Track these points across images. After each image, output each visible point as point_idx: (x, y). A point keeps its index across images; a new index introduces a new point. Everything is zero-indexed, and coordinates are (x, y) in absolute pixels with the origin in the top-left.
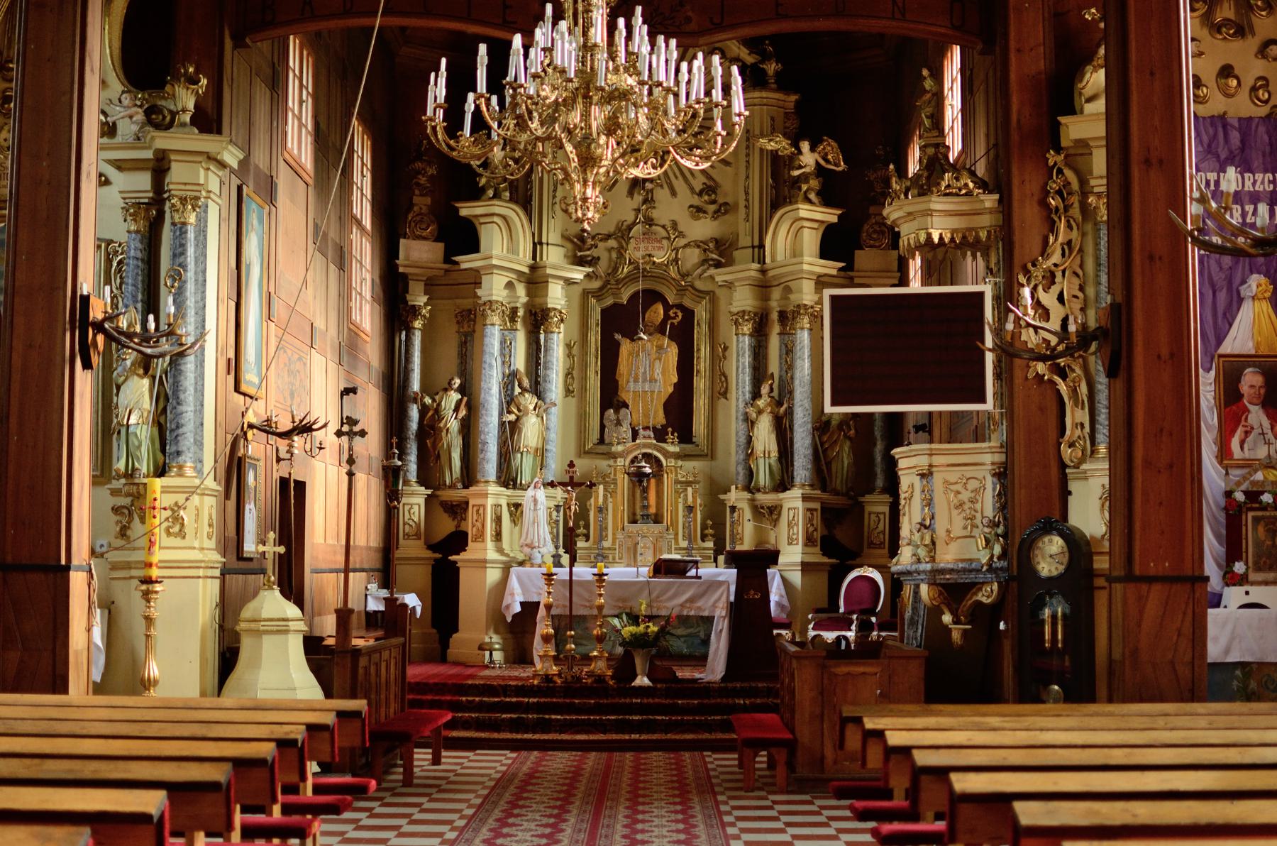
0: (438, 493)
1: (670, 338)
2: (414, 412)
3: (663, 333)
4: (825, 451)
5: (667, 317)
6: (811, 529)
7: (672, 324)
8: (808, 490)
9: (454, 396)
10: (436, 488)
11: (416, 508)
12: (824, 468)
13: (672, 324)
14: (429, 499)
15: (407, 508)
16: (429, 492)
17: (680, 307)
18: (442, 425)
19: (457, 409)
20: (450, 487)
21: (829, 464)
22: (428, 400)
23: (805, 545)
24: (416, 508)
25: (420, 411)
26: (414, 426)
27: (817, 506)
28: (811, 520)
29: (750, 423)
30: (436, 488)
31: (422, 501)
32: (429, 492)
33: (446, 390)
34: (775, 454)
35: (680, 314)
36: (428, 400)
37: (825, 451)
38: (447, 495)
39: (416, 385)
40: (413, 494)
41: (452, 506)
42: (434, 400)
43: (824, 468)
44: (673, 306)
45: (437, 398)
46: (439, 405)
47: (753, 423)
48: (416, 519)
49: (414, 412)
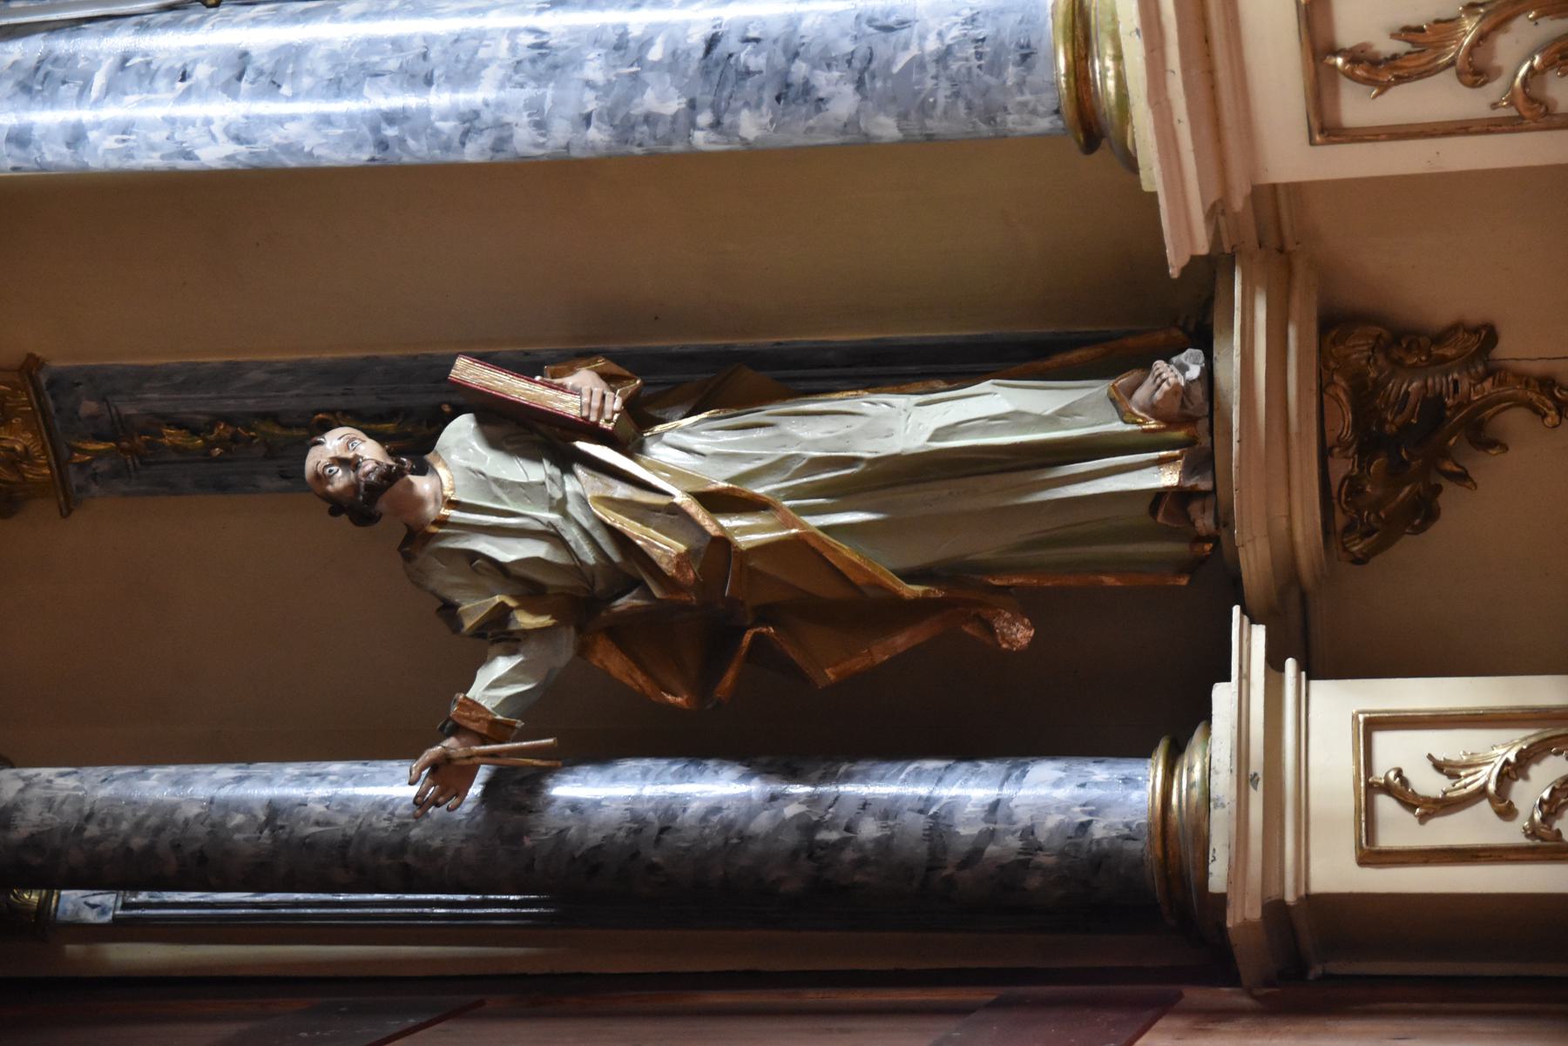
0: (1254, 559)
2: (602, 793)
9: (463, 457)
10: (1226, 586)
11: (1393, 751)
14: (1319, 643)
15: (1398, 828)
16: (1250, 643)
18: (665, 546)
19: (548, 438)
20: (1201, 459)
22: (494, 683)
24: (1399, 753)
25: (600, 751)
26: (717, 789)
30: (1226, 586)
31: (1335, 706)
32: (1250, 643)
33: (418, 537)
36: (494, 683)
38: (1277, 512)
39: (390, 786)
40: (1270, 776)
41: (1368, 441)
42: (497, 634)
45: (474, 608)
46: (525, 583)
48: (1502, 746)
49: (602, 793)
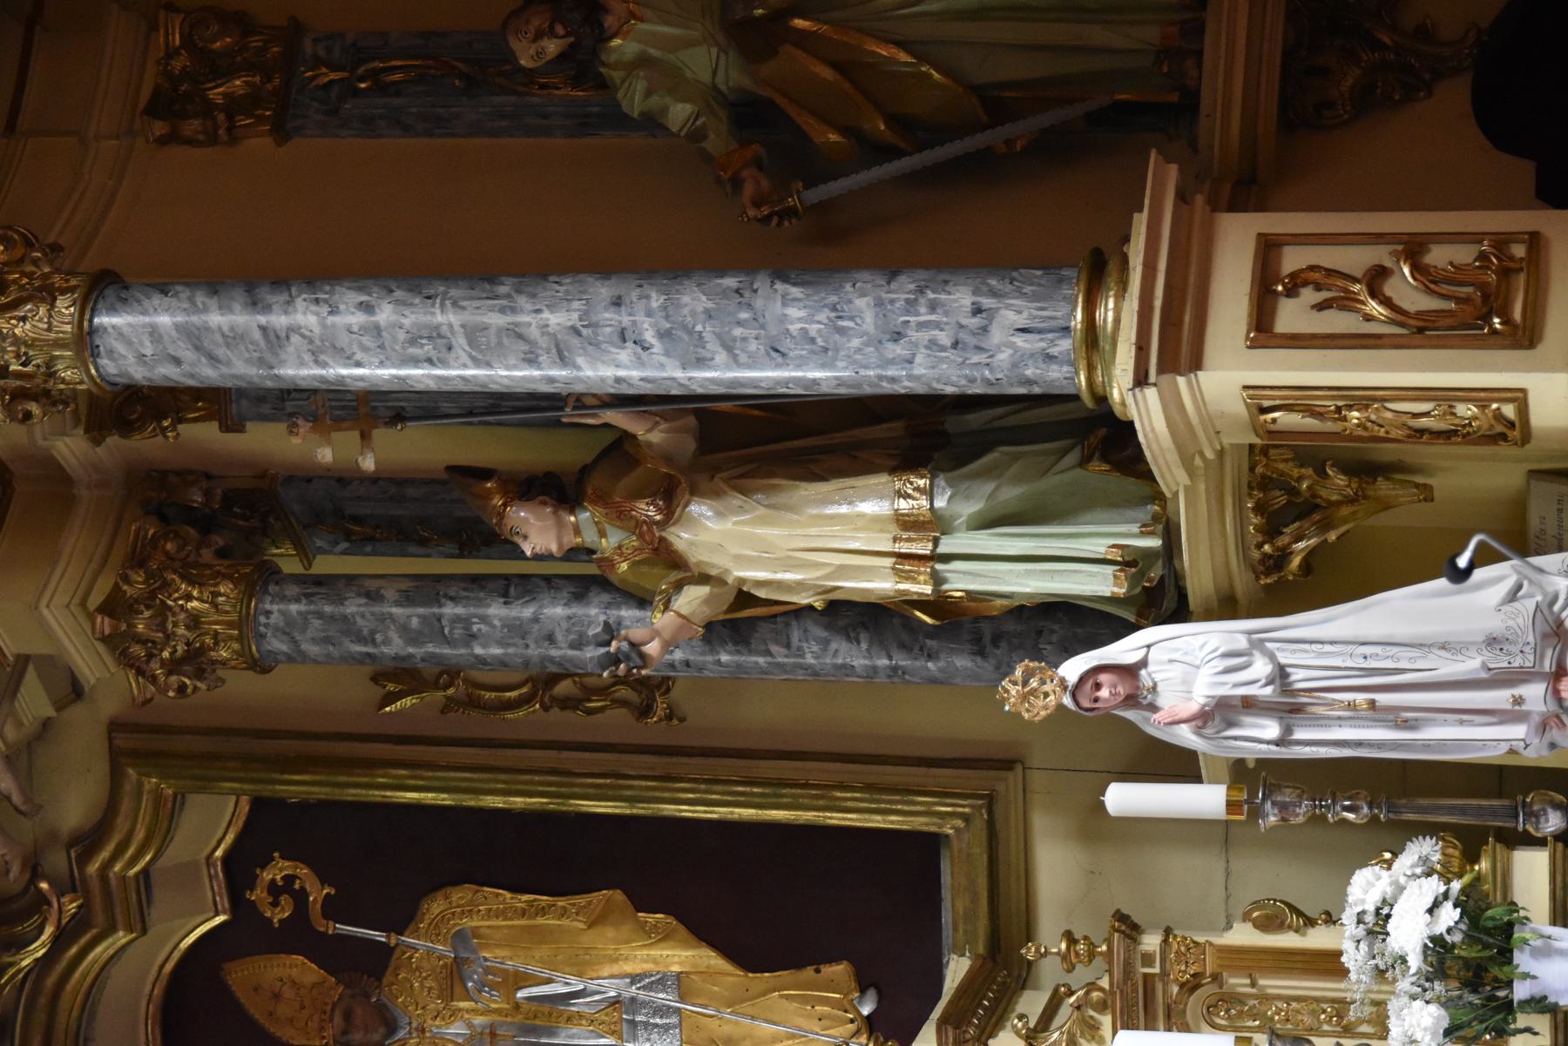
1: (401, 921)
3: (378, 960)
4: (915, 130)
5: (298, 936)
6: (1405, 287)
7: (332, 909)
8: (1119, 314)
12: (1021, 130)
13: (332, 909)
17: (239, 869)
21: (996, 104)
23: (1525, 336)
27: (1235, 246)
28: (1335, 291)
29: (745, 617)
34: (913, 495)
35: (278, 870)
37: (915, 130)
43: (1021, 130)
44: (238, 903)
47: (744, 598)
